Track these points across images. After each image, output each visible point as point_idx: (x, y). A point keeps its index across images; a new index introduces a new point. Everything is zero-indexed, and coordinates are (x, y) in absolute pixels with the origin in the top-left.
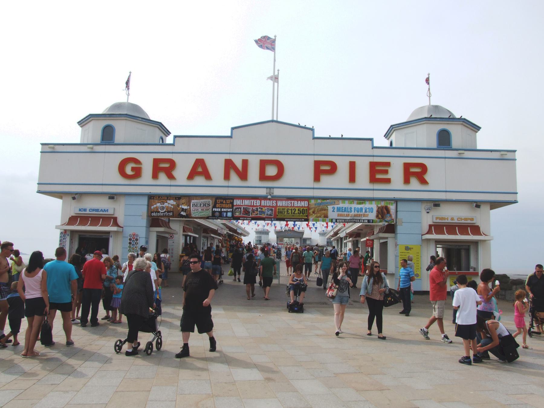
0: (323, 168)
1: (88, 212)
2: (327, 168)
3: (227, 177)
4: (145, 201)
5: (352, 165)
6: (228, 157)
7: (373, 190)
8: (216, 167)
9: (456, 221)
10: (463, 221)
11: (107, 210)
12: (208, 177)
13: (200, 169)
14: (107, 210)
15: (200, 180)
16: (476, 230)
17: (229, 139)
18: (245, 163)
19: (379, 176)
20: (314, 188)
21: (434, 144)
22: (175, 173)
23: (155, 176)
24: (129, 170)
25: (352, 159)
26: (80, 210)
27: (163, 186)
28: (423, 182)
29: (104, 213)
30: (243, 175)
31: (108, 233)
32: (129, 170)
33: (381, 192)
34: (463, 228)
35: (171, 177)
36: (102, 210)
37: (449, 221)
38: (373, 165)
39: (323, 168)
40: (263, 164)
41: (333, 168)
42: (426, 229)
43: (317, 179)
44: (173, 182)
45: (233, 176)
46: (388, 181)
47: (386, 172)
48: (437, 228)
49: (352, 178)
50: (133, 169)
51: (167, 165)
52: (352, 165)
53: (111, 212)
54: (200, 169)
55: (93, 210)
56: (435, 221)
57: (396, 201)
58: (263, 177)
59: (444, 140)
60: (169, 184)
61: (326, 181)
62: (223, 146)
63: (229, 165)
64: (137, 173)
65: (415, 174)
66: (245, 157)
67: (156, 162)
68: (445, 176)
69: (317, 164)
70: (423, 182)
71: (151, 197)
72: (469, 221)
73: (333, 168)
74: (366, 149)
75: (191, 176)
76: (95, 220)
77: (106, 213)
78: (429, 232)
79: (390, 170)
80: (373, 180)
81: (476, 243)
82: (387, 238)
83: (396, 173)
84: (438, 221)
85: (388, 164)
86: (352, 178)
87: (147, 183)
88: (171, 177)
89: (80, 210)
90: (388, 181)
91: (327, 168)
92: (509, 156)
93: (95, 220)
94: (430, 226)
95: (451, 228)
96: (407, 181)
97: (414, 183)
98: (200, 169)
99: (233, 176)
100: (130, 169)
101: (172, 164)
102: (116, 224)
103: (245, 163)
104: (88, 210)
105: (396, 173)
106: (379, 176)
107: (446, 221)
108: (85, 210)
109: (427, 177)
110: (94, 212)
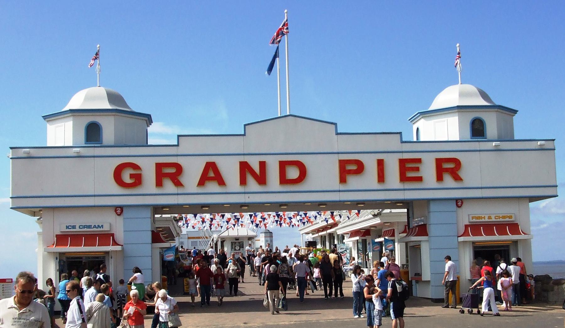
0: (349, 168)
1: (77, 229)
2: (354, 167)
3: (243, 182)
4: (148, 213)
5: (380, 163)
6: (243, 159)
7: (404, 190)
8: (230, 170)
9: (493, 220)
10: (501, 220)
11: (102, 226)
12: (221, 182)
13: (211, 174)
14: (102, 226)
15: (212, 187)
16: (514, 228)
17: (242, 137)
18: (263, 165)
19: (410, 174)
20: (339, 191)
21: (468, 135)
22: (183, 179)
23: (159, 183)
24: (127, 179)
25: (381, 156)
26: (67, 227)
27: (169, 194)
28: (457, 178)
29: (99, 229)
30: (261, 179)
31: (107, 253)
32: (127, 179)
33: (412, 194)
34: (501, 227)
35: (178, 184)
36: (95, 227)
37: (487, 220)
38: (402, 162)
39: (349, 168)
40: (283, 165)
41: (360, 168)
42: (462, 230)
43: (343, 180)
44: (180, 190)
45: (250, 180)
46: (420, 179)
47: (417, 169)
48: (474, 228)
49: (381, 178)
50: (132, 176)
51: (172, 170)
52: (380, 163)
53: (106, 228)
54: (211, 174)
55: (84, 227)
56: (471, 220)
57: (428, 201)
58: (284, 180)
59: (478, 129)
60: (176, 192)
61: (354, 182)
62: (235, 146)
63: (245, 167)
64: (138, 180)
65: (447, 170)
66: (263, 159)
67: (159, 166)
68: (482, 170)
69: (343, 164)
70: (457, 178)
71: (158, 209)
72: (507, 219)
73: (360, 168)
74: (393, 143)
75: (201, 183)
76: (90, 238)
77: (101, 229)
78: (465, 234)
79: (422, 167)
80: (403, 178)
81: (516, 242)
82: (420, 241)
83: (428, 171)
84: (474, 220)
85: (419, 161)
86: (381, 178)
87: (150, 192)
88: (178, 184)
89: (67, 227)
90: (420, 179)
91: (354, 167)
92: (549, 145)
93: (90, 238)
94: (466, 226)
95: (489, 228)
96: (440, 178)
97: (448, 181)
98: (211, 174)
99: (250, 180)
100: (127, 176)
101: (179, 168)
102: (115, 243)
103: (263, 165)
104: (77, 227)
105: (428, 171)
106: (410, 174)
107: (483, 220)
108: (74, 227)
109: (462, 173)
110: (86, 229)
